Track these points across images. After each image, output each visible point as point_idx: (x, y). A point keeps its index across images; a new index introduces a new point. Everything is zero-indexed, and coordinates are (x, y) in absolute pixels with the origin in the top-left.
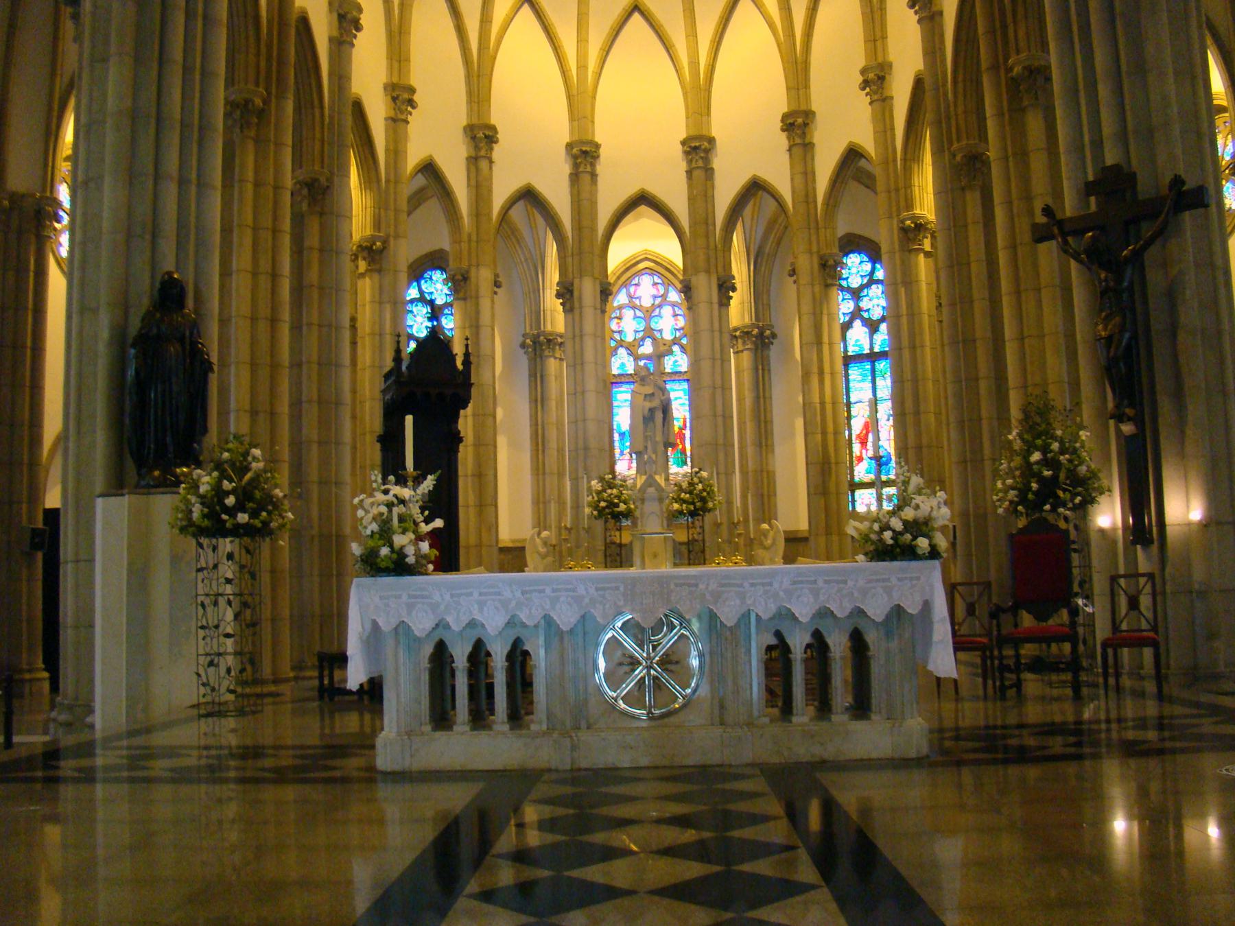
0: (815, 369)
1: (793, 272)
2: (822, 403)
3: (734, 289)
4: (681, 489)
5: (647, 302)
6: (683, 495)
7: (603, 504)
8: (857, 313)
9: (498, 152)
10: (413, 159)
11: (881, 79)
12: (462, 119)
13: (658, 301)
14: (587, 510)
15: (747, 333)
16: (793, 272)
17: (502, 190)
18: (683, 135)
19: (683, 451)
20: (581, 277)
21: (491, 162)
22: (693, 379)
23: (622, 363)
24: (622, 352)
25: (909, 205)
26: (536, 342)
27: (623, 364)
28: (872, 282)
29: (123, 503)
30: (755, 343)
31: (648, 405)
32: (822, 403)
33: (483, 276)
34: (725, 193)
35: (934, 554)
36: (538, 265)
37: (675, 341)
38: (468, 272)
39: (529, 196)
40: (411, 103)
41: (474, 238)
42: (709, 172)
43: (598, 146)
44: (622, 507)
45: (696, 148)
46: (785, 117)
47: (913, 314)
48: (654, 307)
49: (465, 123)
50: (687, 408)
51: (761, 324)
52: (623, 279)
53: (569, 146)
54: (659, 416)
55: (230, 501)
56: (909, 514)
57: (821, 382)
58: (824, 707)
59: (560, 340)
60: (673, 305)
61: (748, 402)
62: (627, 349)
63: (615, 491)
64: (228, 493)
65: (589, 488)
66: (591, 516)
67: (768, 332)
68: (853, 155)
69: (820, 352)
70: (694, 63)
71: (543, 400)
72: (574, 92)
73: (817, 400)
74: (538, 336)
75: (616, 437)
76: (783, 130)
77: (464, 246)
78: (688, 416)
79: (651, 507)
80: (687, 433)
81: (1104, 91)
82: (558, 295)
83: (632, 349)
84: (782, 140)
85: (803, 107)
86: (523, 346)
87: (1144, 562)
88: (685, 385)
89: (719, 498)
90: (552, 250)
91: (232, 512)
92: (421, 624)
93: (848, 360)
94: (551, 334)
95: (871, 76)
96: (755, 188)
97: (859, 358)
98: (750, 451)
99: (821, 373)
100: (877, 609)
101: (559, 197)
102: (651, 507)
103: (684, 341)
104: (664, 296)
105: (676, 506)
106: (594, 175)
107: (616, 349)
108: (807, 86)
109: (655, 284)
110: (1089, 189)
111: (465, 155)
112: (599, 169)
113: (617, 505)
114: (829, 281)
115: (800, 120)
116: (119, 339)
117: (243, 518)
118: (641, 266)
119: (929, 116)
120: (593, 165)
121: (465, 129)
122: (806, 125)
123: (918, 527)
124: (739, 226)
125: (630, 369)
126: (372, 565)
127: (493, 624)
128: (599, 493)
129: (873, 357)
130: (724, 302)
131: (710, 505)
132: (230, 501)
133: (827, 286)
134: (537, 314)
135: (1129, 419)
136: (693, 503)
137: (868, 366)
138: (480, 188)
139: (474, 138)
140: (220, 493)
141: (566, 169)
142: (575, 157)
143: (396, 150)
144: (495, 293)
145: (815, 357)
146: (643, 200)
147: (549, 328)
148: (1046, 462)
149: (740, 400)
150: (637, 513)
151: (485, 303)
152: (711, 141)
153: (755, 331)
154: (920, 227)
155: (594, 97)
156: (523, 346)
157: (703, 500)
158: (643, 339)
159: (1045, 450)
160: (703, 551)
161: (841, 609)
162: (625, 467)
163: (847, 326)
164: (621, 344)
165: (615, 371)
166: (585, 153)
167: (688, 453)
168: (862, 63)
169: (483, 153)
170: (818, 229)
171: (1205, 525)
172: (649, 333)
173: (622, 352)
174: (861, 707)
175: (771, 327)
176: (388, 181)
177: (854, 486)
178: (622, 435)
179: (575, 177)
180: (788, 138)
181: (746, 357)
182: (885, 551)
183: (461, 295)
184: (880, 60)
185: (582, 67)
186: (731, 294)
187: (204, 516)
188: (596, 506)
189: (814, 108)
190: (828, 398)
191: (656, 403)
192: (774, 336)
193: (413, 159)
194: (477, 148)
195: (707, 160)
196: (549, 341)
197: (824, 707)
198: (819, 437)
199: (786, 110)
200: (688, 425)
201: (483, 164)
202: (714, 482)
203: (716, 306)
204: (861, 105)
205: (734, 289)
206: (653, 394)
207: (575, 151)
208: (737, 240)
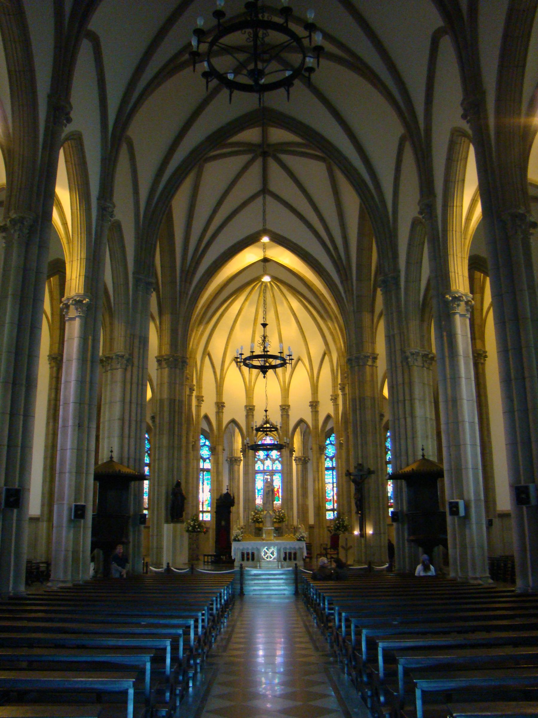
0: (317, 479)
1: (311, 449)
2: (319, 489)
3: (294, 451)
4: (276, 516)
6: (277, 517)
7: (255, 519)
9: (225, 410)
10: (202, 414)
12: (215, 400)
14: (250, 520)
15: (300, 459)
16: (311, 449)
17: (225, 421)
18: (280, 404)
19: (279, 496)
21: (223, 412)
22: (282, 472)
23: (259, 466)
24: (259, 462)
26: (231, 460)
27: (259, 466)
29: (172, 525)
30: (302, 462)
31: (268, 489)
32: (319, 489)
33: (220, 448)
34: (292, 423)
35: (304, 541)
36: (233, 434)
37: (277, 459)
38: (215, 447)
39: (233, 421)
40: (203, 401)
41: (218, 436)
42: (288, 416)
43: (254, 406)
44: (260, 520)
45: (284, 408)
46: (310, 402)
50: (280, 482)
51: (305, 456)
52: (260, 437)
53: (246, 406)
54: (271, 493)
55: (197, 527)
56: (301, 535)
57: (318, 483)
59: (239, 459)
61: (300, 481)
62: (261, 461)
63: (258, 515)
64: (196, 525)
65: (251, 514)
66: (251, 522)
67: (307, 459)
68: (328, 417)
69: (318, 474)
70: (284, 382)
71: (233, 479)
72: (248, 389)
73: (317, 487)
74: (232, 458)
75: (256, 491)
76: (310, 406)
77: (215, 439)
78: (281, 484)
79: (268, 519)
80: (280, 490)
83: (262, 462)
84: (310, 409)
85: (316, 400)
86: (227, 460)
87: (363, 541)
88: (280, 474)
89: (287, 518)
90: (237, 430)
91: (197, 528)
92: (241, 548)
94: (237, 457)
95: (333, 398)
96: (301, 421)
98: (300, 497)
99: (318, 480)
100: (297, 547)
101: (242, 422)
102: (268, 519)
103: (280, 459)
105: (275, 520)
106: (253, 415)
107: (257, 461)
108: (317, 393)
109: (271, 440)
110: (355, 468)
112: (255, 413)
113: (259, 519)
114: (322, 453)
115: (314, 404)
116: (167, 493)
117: (199, 530)
120: (253, 412)
122: (316, 405)
123: (303, 537)
124: (299, 428)
125: (262, 469)
126: (235, 540)
127: (250, 548)
128: (254, 516)
130: (291, 455)
131: (284, 520)
132: (197, 527)
133: (321, 454)
134: (232, 450)
135: (360, 514)
136: (279, 519)
140: (195, 525)
141: (244, 413)
142: (247, 410)
143: (198, 414)
144: (223, 452)
145: (317, 476)
147: (235, 455)
148: (339, 523)
149: (297, 480)
150: (264, 522)
151: (220, 456)
152: (289, 406)
153: (303, 458)
155: (253, 390)
156: (227, 460)
157: (283, 519)
159: (339, 521)
160: (282, 532)
161: (292, 547)
162: (259, 501)
164: (259, 460)
165: (256, 469)
166: (250, 409)
167: (280, 497)
168: (331, 393)
169: (220, 411)
170: (319, 436)
171: (373, 534)
173: (259, 462)
175: (308, 457)
176: (196, 424)
177: (333, 510)
178: (258, 490)
179: (247, 416)
180: (311, 408)
181: (300, 466)
182: (299, 540)
183: (214, 454)
184: (336, 393)
185: (250, 382)
186: (294, 453)
187: (192, 529)
188: (252, 519)
190: (320, 488)
191: (270, 489)
192: (309, 459)
193: (202, 414)
196: (236, 460)
198: (317, 499)
199: (311, 400)
200: (280, 487)
201: (221, 414)
202: (286, 513)
203: (289, 457)
205: (294, 451)
206: (269, 486)
207: (248, 408)
208: (298, 430)
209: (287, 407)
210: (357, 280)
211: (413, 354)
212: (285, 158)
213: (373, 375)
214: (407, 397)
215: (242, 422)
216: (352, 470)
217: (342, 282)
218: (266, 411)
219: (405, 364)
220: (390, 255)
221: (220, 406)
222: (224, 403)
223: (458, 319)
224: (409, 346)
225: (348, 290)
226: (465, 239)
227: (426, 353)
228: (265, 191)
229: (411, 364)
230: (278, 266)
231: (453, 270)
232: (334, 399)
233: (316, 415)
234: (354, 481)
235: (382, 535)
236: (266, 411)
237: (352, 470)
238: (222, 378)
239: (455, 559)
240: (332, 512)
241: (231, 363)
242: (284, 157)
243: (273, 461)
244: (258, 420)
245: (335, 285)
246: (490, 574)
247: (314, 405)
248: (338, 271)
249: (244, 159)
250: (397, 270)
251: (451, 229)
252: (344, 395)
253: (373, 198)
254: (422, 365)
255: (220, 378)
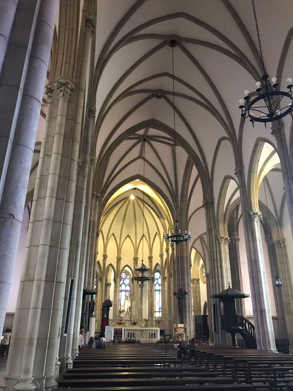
5: (124, 277)
8: (157, 283)
9: (107, 259)
11: (162, 256)
12: (103, 254)
13: (126, 277)
18: (134, 257)
20: (117, 278)
25: (165, 275)
28: (160, 278)
37: (128, 285)
39: (111, 265)
47: (164, 290)
48: (125, 278)
49: (103, 254)
58: (152, 338)
60: (128, 278)
68: (157, 264)
70: (136, 246)
72: (118, 248)
76: (148, 259)
81: (180, 280)
82: (113, 280)
85: (151, 256)
93: (155, 291)
97: (157, 290)
101: (115, 266)
103: (129, 285)
104: (127, 277)
106: (120, 262)
108: (152, 252)
109: (125, 274)
110: (178, 291)
111: (103, 259)
112: (121, 261)
118: (123, 271)
119: (167, 267)
121: (103, 255)
122: (151, 258)
129: (159, 290)
137: (159, 291)
138: (104, 264)
139: (104, 257)
141: (116, 261)
146: (127, 266)
152: (138, 258)
154: (166, 277)
155: (121, 249)
158: (123, 284)
163: (155, 285)
168: (160, 253)
172: (124, 283)
174: (155, 338)
189: (153, 256)
194: (104, 258)
195: (137, 261)
197: (152, 338)
201: (105, 261)
204: (159, 258)
207: (118, 258)
209: (137, 259)
210: (180, 201)
211: (221, 238)
212: (154, 143)
213: (187, 246)
214: (218, 258)
215: (115, 266)
216: (176, 292)
217: (173, 202)
218: (142, 261)
219: (217, 242)
220: (209, 191)
221: (105, 257)
222: (107, 255)
223: (256, 223)
224: (219, 234)
225: (176, 206)
226: (257, 187)
227: (227, 237)
228: (141, 157)
229: (220, 242)
230: (139, 191)
231: (253, 201)
232: (161, 256)
233: (151, 263)
234: (177, 297)
235: (191, 326)
236: (142, 261)
237: (176, 292)
238: (107, 243)
239: (260, 340)
240: (159, 313)
241: (111, 236)
242: (153, 143)
243: (126, 286)
244: (139, 266)
245: (170, 202)
246: (276, 349)
247: (150, 258)
248: (172, 196)
249: (136, 141)
250: (213, 199)
251: (252, 182)
252: (168, 254)
253: (202, 165)
254: (224, 243)
255: (106, 243)
